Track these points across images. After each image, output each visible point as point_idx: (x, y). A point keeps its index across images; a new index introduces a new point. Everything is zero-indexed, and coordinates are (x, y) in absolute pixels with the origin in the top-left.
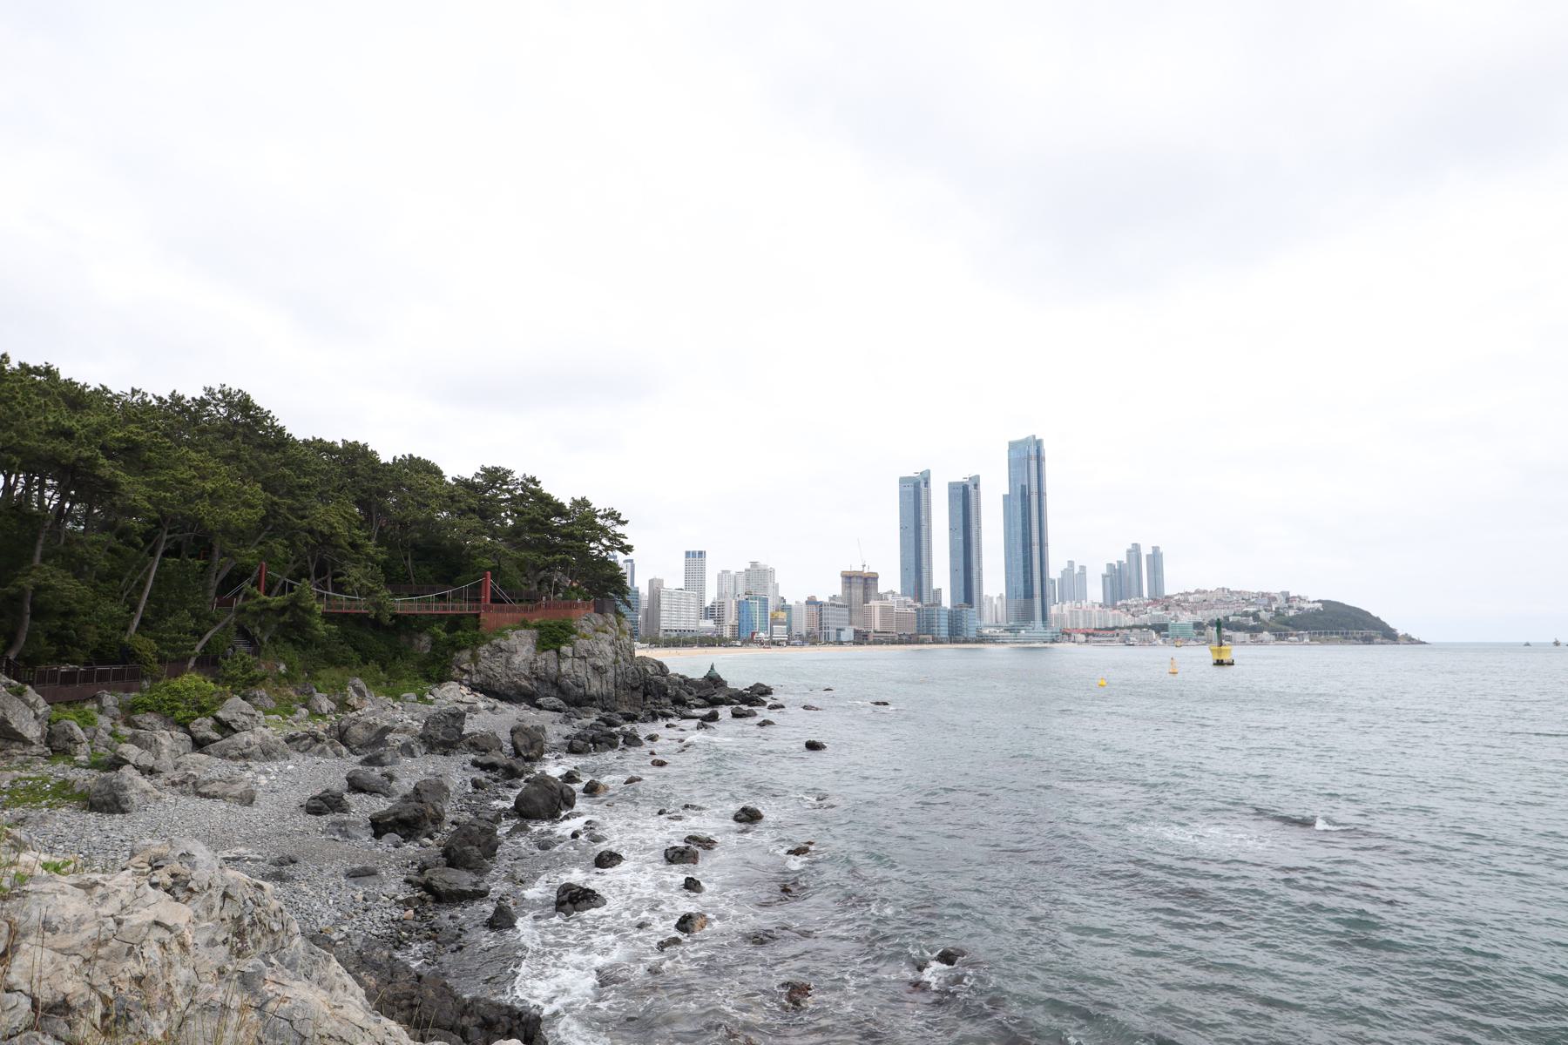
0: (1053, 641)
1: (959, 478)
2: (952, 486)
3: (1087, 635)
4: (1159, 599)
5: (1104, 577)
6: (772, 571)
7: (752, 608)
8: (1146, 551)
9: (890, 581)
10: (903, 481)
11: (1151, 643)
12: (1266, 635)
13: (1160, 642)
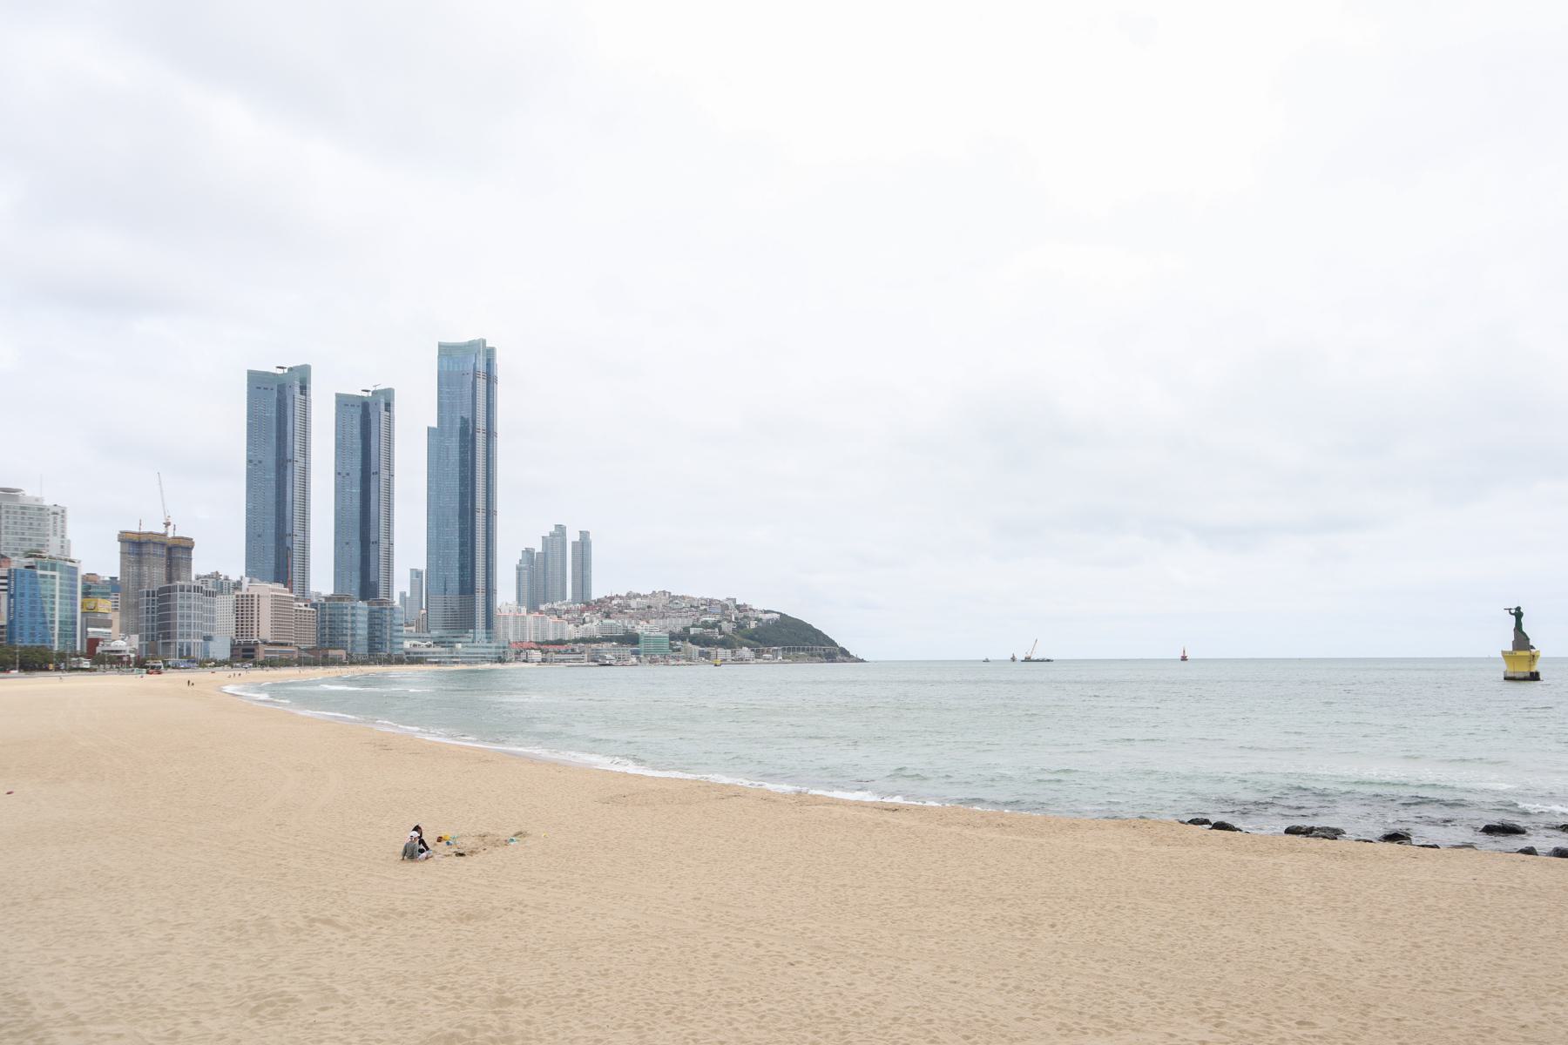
0: (501, 660)
1: (356, 388)
2: (343, 402)
4: (589, 606)
5: (519, 569)
6: (59, 514)
7: (44, 589)
8: (572, 536)
9: (221, 550)
10: (259, 383)
11: (621, 661)
12: (745, 652)
13: (634, 660)
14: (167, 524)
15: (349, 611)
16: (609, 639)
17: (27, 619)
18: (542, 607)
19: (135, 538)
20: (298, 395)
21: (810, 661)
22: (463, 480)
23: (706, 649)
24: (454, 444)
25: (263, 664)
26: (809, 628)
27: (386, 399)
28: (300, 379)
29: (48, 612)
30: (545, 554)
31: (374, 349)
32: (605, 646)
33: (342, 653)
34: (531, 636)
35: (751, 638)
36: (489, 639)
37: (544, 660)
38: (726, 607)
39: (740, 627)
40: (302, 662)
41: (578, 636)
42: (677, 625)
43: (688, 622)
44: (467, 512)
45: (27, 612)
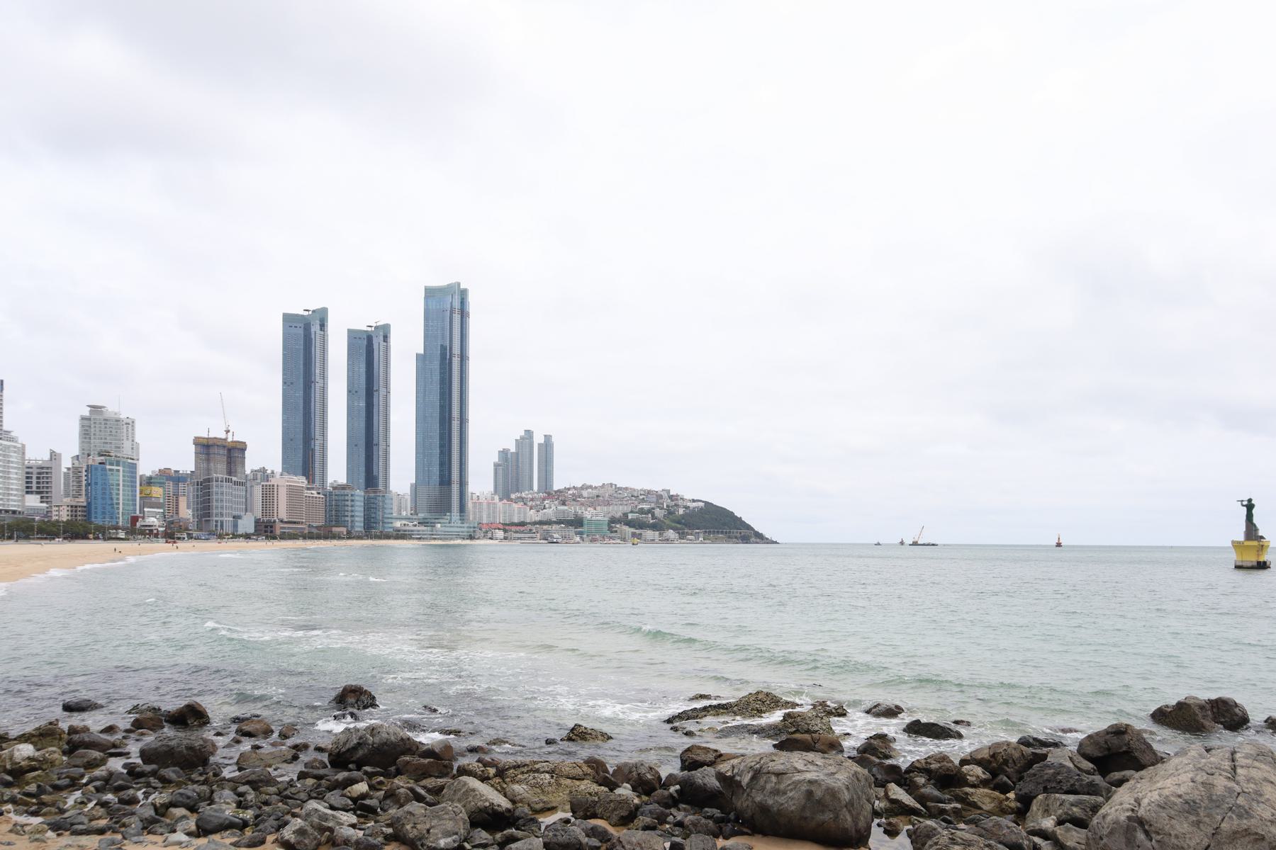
0: (471, 538)
1: (362, 324)
2: (353, 335)
3: (505, 531)
4: (550, 494)
5: (496, 465)
6: (131, 424)
7: (111, 479)
8: (538, 439)
10: (290, 320)
12: (671, 534)
13: (578, 539)
14: (228, 432)
15: (349, 498)
16: (559, 522)
17: (99, 501)
18: (513, 496)
19: (205, 442)
20: (318, 332)
21: (727, 542)
22: (442, 394)
23: (638, 531)
24: (436, 365)
25: (283, 537)
26: (730, 515)
27: (384, 332)
28: (321, 317)
29: (114, 496)
30: (517, 454)
31: (378, 295)
32: (555, 527)
33: (344, 530)
34: (501, 519)
35: (679, 522)
36: (462, 520)
37: (505, 538)
38: (660, 497)
39: (670, 513)
40: (310, 537)
41: (538, 519)
42: (617, 511)
43: (627, 509)
44: (445, 420)
45: (99, 496)
